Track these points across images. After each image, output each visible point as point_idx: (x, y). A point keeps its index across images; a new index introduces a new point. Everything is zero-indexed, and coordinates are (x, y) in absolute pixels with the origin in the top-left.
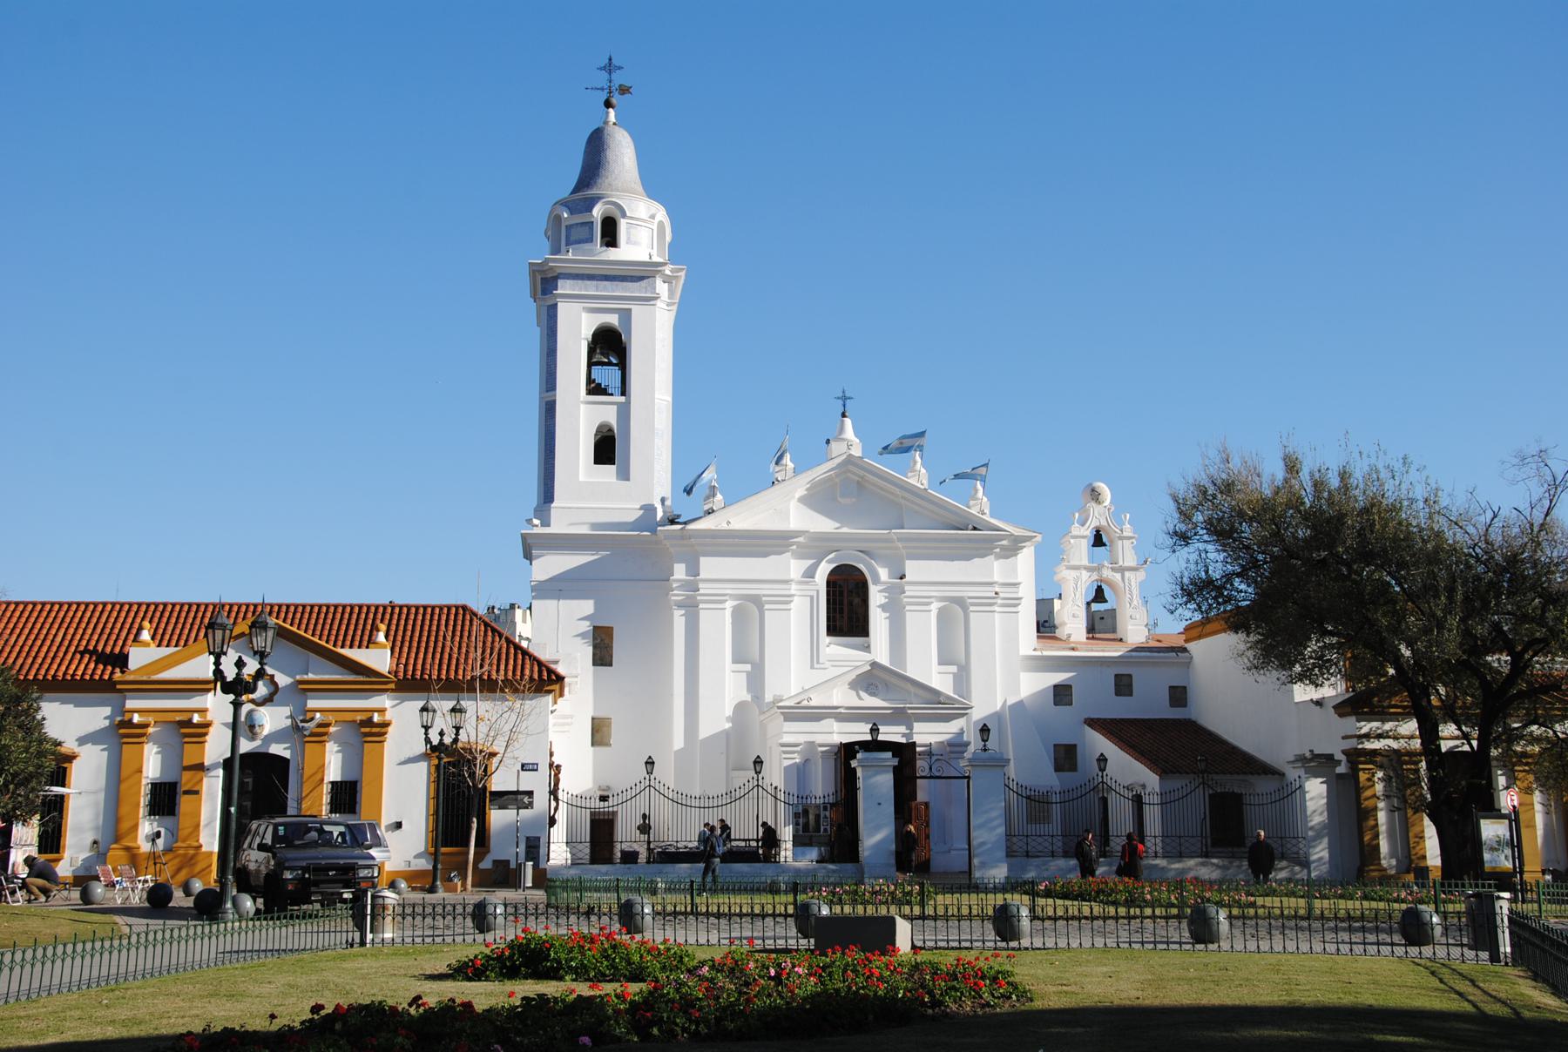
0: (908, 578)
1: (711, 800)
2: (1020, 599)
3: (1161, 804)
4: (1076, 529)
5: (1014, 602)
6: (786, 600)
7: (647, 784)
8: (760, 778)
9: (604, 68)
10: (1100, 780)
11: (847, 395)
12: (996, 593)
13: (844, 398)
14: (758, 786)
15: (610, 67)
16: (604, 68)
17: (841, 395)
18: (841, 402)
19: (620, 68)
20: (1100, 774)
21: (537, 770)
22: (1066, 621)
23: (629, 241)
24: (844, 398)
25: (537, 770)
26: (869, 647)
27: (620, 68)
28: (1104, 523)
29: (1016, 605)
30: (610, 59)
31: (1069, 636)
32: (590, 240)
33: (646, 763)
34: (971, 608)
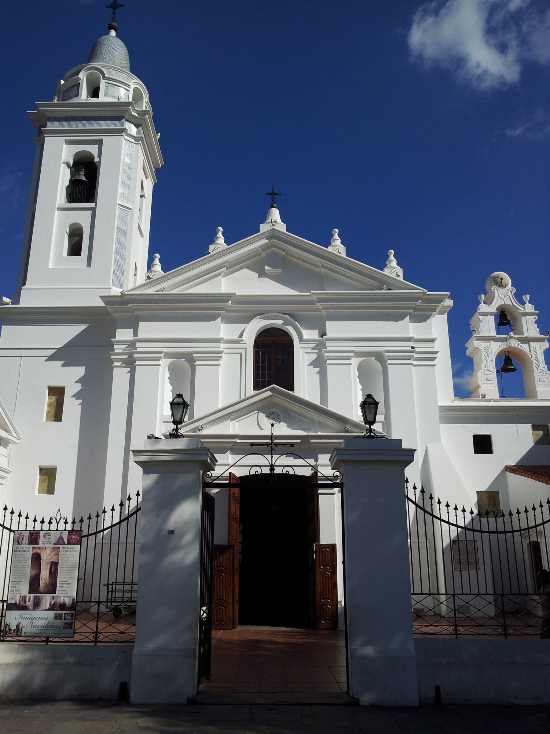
0: (329, 335)
2: (436, 353)
4: (483, 308)
5: (431, 356)
6: (216, 356)
9: (111, 7)
11: (276, 191)
12: (412, 348)
16: (111, 7)
17: (270, 191)
19: (122, 6)
22: (480, 384)
23: (106, 94)
27: (122, 6)
28: (508, 302)
29: (433, 359)
31: (484, 396)
34: (389, 362)
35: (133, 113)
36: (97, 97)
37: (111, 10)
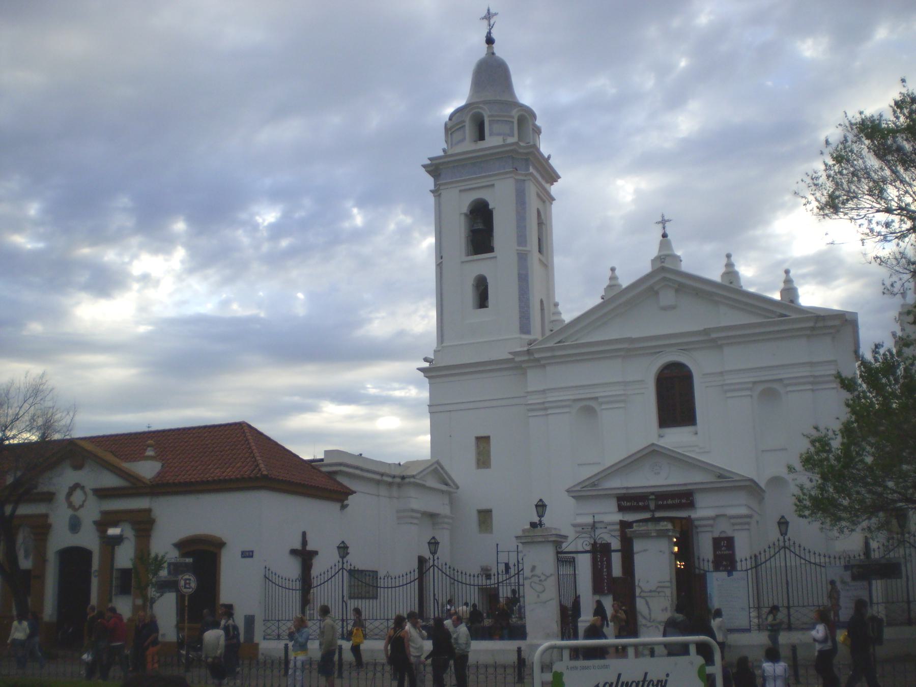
1: (476, 578)
3: (377, 587)
7: (341, 567)
8: (436, 558)
10: (782, 544)
11: (666, 218)
13: (663, 222)
14: (434, 565)
15: (489, 16)
17: (660, 219)
18: (661, 226)
20: (781, 538)
21: (252, 556)
24: (663, 222)
25: (252, 556)
26: (696, 433)
27: (496, 14)
30: (489, 10)
32: (463, 140)
33: (339, 548)
35: (521, 151)
36: (481, 137)
37: (485, 22)
